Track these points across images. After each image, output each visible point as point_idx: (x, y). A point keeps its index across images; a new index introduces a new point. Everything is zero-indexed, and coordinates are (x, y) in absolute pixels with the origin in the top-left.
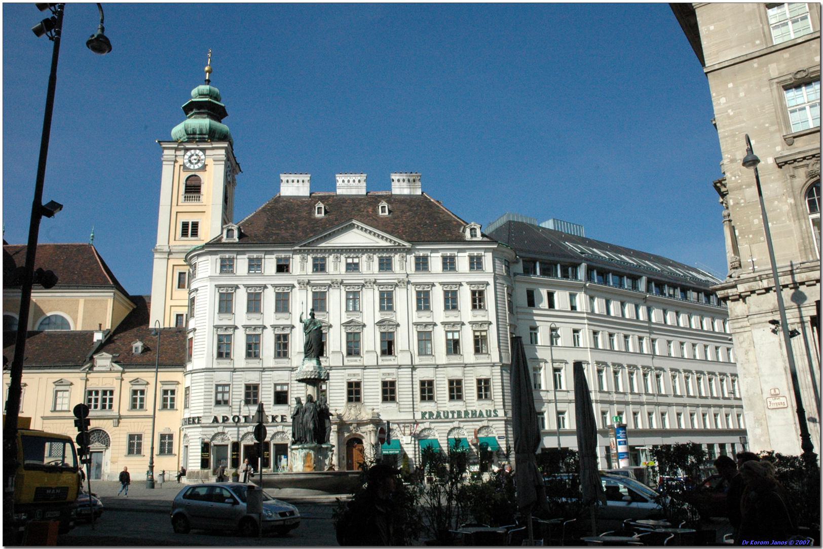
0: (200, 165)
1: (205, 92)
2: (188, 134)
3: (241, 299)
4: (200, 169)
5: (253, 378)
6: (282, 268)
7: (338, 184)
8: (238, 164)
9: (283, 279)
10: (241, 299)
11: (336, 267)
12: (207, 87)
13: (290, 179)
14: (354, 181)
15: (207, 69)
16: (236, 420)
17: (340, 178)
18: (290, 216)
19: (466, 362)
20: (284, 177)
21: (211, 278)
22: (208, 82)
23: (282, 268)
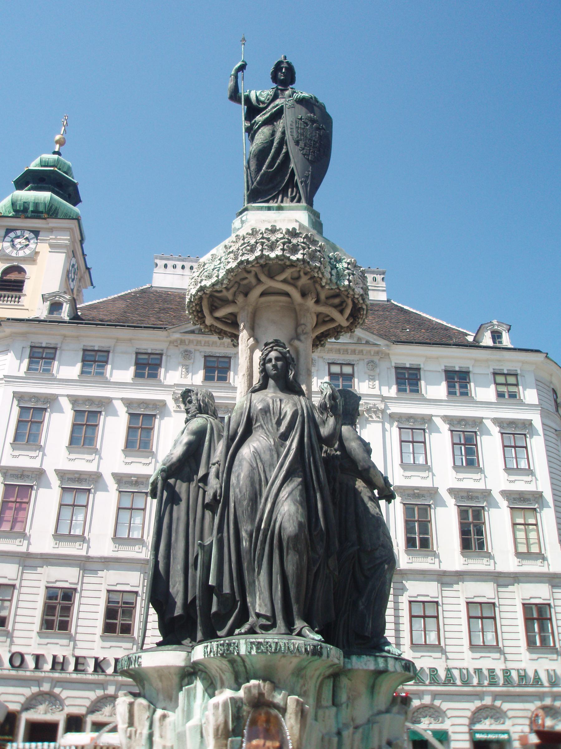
0: (27, 251)
2: (15, 211)
3: (58, 426)
4: (25, 259)
8: (88, 269)
10: (58, 426)
12: (56, 156)
15: (58, 137)
16: (17, 663)
18: (166, 306)
19: (500, 568)
21: (9, 379)
22: (58, 153)
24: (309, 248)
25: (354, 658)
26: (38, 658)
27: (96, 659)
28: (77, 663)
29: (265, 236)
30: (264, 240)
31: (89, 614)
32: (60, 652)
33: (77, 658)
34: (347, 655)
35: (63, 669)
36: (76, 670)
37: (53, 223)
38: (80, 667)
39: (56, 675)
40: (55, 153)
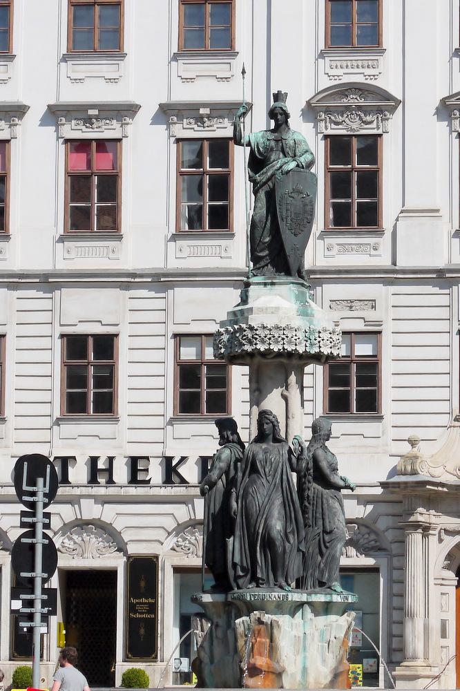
5: (87, 311)
24: (287, 337)
25: (313, 595)
27: (168, 460)
29: (257, 332)
30: (257, 336)
31: (145, 379)
33: (134, 461)
34: (309, 594)
35: (110, 481)
38: (140, 477)
39: (101, 491)
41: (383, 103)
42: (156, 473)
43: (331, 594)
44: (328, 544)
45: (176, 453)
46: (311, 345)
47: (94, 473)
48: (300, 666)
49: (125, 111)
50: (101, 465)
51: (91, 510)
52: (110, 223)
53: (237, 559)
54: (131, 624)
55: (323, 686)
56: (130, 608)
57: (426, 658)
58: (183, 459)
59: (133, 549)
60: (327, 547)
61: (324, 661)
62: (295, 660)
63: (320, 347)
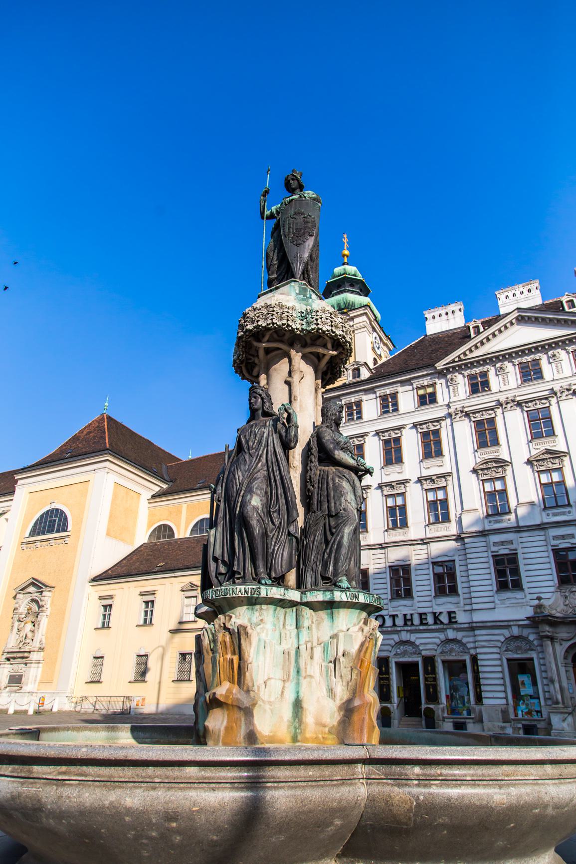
1: (342, 272)
6: (427, 399)
7: (500, 303)
9: (430, 413)
11: (505, 381)
13: (436, 314)
14: (522, 293)
17: (501, 297)
20: (428, 314)
23: (427, 399)
26: (394, 617)
27: (434, 614)
28: (421, 619)
32: (408, 611)
35: (412, 624)
36: (422, 624)
37: (352, 314)
39: (409, 628)
40: (344, 264)
41: (502, 463)
42: (430, 620)
43: (332, 591)
44: (334, 530)
45: (437, 610)
46: (308, 323)
47: (405, 620)
48: (290, 697)
49: (404, 482)
50: (408, 617)
51: (405, 636)
52: (404, 524)
53: (218, 553)
54: (427, 687)
55: (327, 730)
56: (426, 679)
57: (563, 703)
58: (441, 613)
59: (424, 653)
60: (332, 534)
61: (331, 692)
62: (283, 688)
63: (317, 324)
